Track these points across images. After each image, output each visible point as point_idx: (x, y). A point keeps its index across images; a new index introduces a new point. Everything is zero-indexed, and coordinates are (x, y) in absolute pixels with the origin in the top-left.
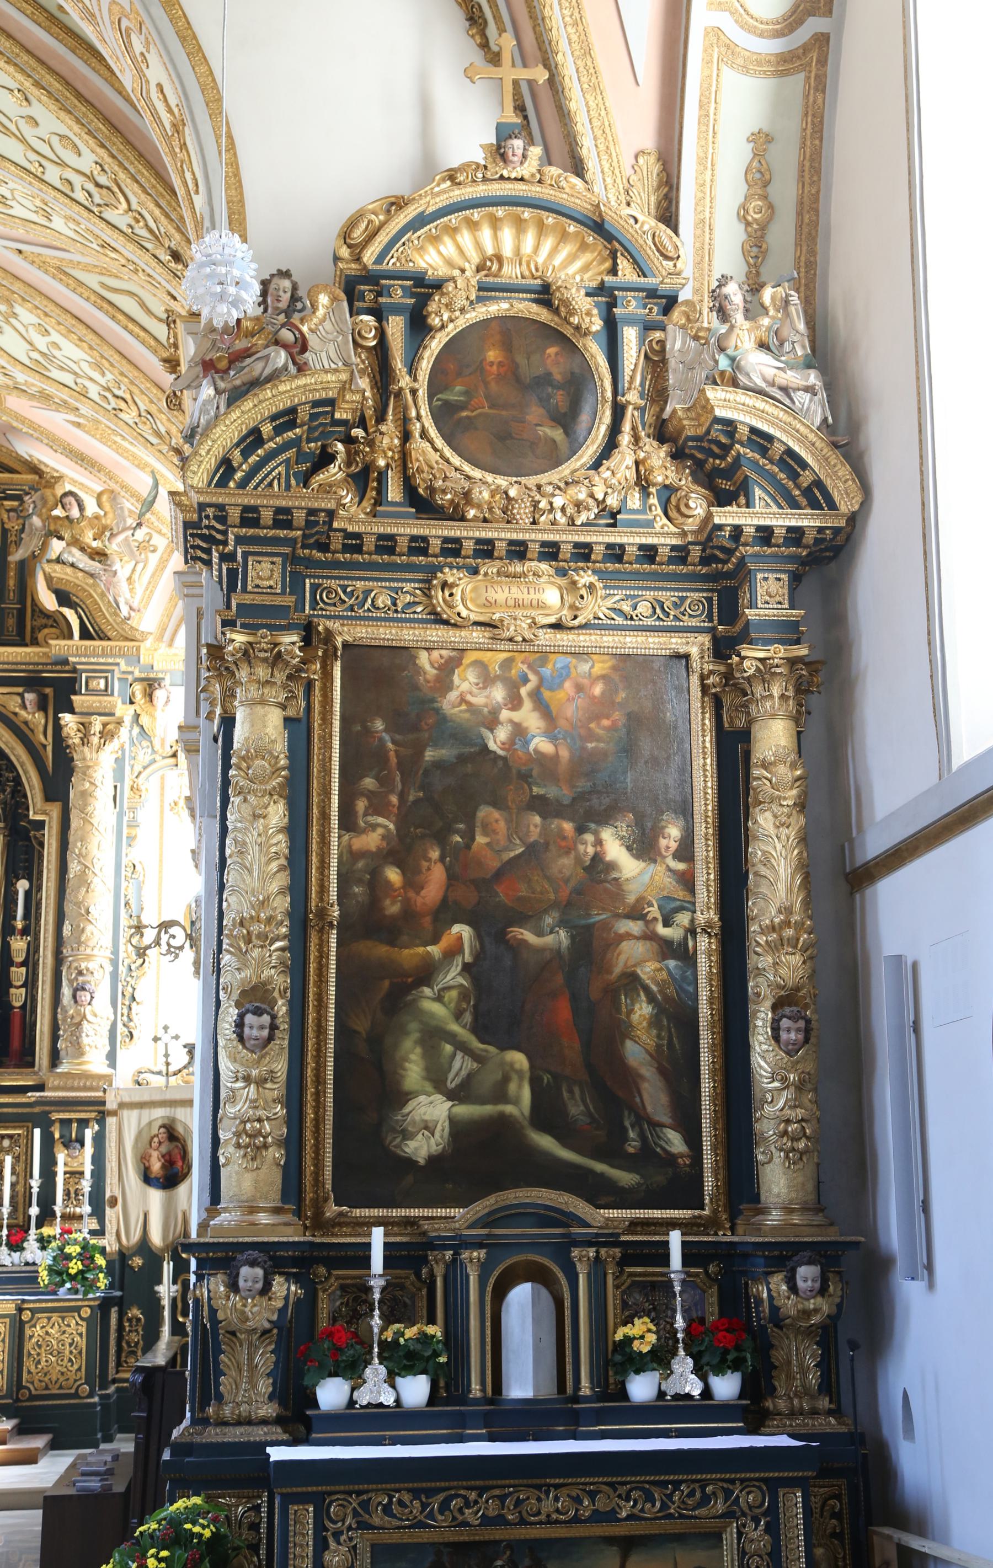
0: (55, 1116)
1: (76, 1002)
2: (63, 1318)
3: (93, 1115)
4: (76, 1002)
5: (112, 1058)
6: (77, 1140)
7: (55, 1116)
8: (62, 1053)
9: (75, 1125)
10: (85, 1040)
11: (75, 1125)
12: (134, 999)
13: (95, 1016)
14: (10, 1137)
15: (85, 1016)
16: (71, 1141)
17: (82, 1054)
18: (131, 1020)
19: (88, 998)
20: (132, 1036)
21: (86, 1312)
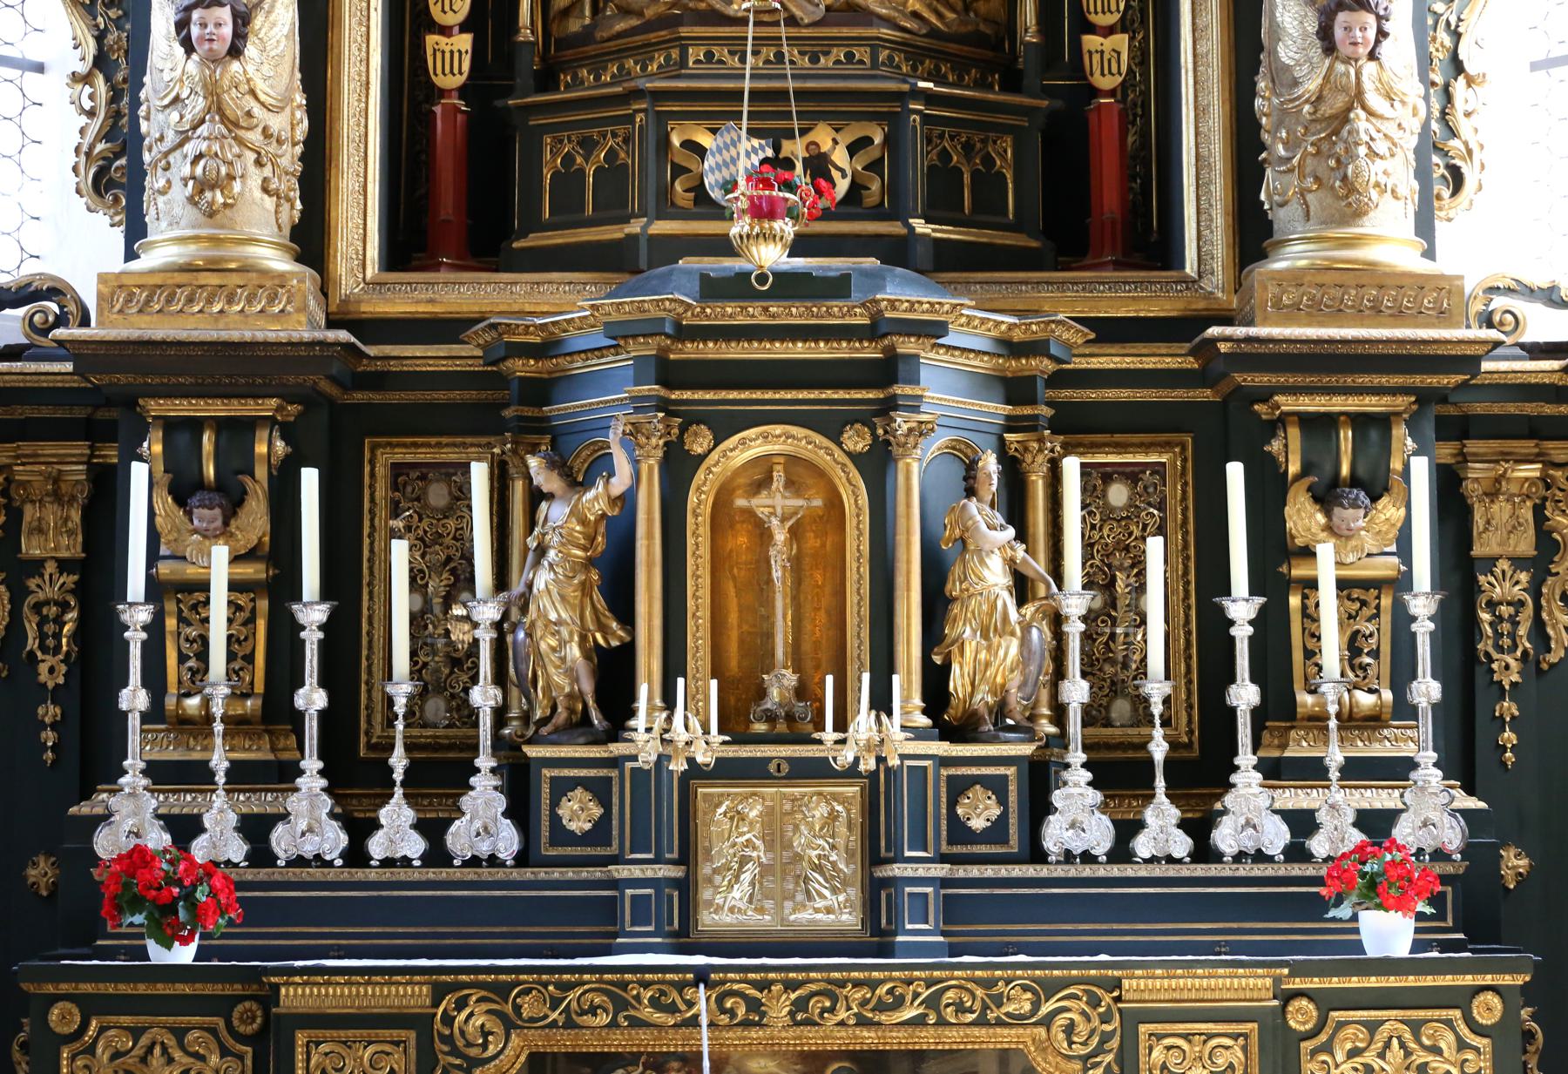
0: (1287, 403)
1: (1329, 47)
2: (1416, 1027)
3: (1402, 402)
4: (1329, 47)
5: (1425, 226)
6: (1355, 481)
7: (1287, 403)
8: (1285, 218)
9: (1346, 436)
10: (1373, 171)
11: (1346, 436)
12: (1457, 66)
13: (1389, 97)
14: (1131, 475)
15: (1359, 94)
16: (1335, 481)
17: (1358, 214)
18: (1453, 133)
19: (1371, 34)
20: (1456, 179)
21: (1489, 1009)
